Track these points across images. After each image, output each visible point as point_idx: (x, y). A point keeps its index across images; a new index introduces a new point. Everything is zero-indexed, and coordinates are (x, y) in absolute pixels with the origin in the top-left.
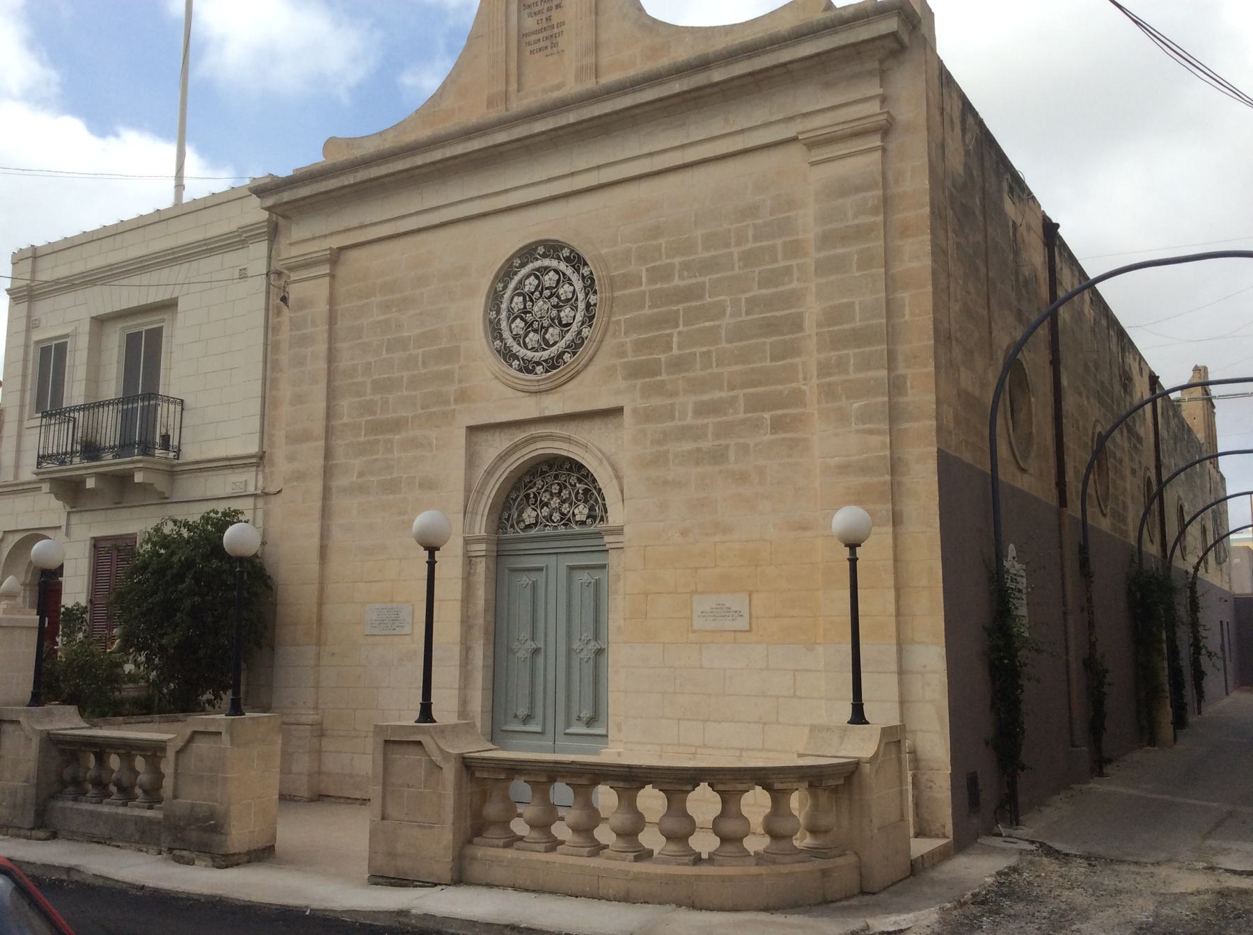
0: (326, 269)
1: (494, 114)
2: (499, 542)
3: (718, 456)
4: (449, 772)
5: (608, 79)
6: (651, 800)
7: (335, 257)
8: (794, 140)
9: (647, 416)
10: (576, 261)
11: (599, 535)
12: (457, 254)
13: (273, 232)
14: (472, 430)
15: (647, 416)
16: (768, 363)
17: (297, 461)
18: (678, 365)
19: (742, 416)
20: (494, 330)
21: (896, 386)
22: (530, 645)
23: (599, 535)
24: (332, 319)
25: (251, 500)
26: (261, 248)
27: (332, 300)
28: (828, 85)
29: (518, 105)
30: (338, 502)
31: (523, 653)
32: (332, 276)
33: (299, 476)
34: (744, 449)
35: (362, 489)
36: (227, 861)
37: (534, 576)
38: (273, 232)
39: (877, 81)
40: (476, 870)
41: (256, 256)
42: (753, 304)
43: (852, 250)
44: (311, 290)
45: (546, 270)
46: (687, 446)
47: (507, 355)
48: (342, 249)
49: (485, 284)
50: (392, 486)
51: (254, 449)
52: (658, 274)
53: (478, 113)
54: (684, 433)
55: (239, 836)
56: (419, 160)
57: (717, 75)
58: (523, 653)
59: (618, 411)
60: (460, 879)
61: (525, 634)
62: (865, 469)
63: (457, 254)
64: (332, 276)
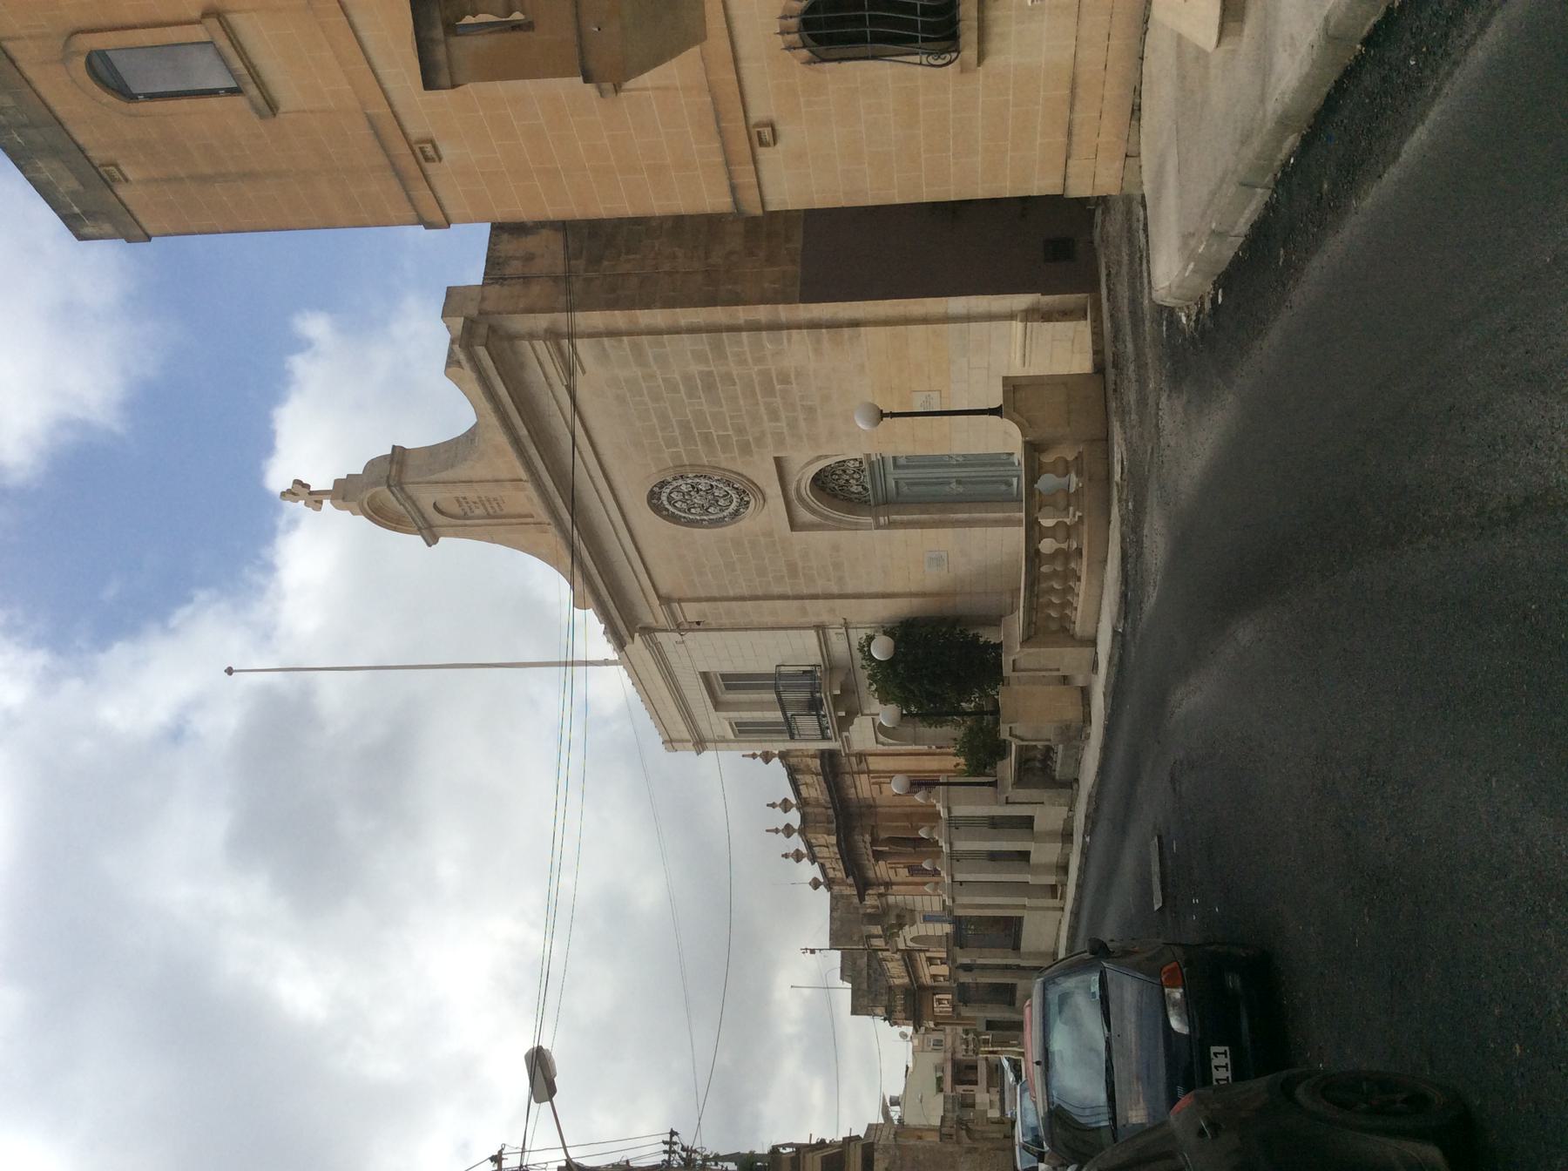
0: (675, 605)
1: (553, 530)
2: (877, 505)
3: (810, 410)
4: (1027, 650)
5: (523, 474)
6: (1047, 546)
7: (665, 600)
8: (568, 387)
9: (780, 441)
10: (663, 484)
11: (871, 464)
12: (663, 551)
13: (647, 631)
14: (794, 526)
15: (780, 441)
16: (738, 388)
17: (819, 611)
18: (740, 430)
19: (778, 399)
20: (719, 523)
21: (754, 327)
22: (954, 485)
23: (871, 464)
24: (708, 599)
25: (851, 631)
26: (660, 637)
27: (698, 600)
28: (522, 366)
29: (543, 516)
30: (849, 590)
31: (961, 489)
32: (680, 601)
33: (832, 611)
34: (802, 398)
35: (841, 579)
36: (1087, 719)
37: (902, 483)
38: (647, 631)
39: (517, 342)
40: (1089, 631)
41: (667, 640)
42: (690, 396)
43: (649, 354)
44: (691, 612)
45: (669, 499)
46: (802, 424)
47: (736, 514)
48: (659, 597)
49: (682, 530)
50: (837, 566)
51: (813, 633)
52: (671, 443)
53: (552, 537)
54: (792, 425)
55: (1072, 713)
56: (594, 571)
57: (523, 432)
58: (961, 489)
59: (779, 462)
60: (1093, 642)
61: (947, 488)
62: (818, 341)
63: (663, 551)
64: (680, 601)
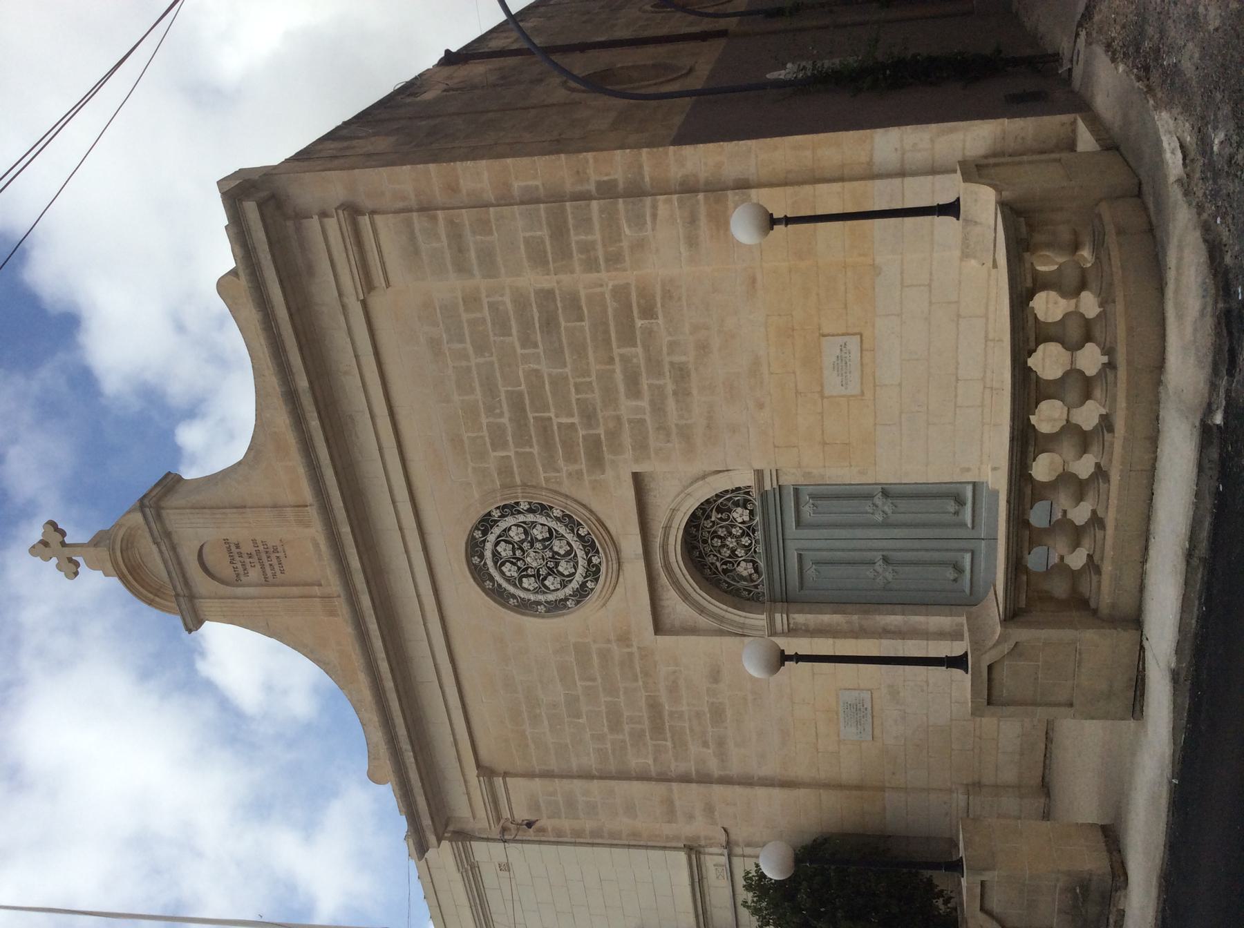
0: (499, 781)
1: (342, 606)
2: (773, 600)
3: (681, 374)
4: (1022, 634)
5: (307, 494)
7: (486, 772)
8: (364, 303)
9: (641, 447)
10: (486, 523)
11: (764, 495)
13: (462, 836)
14: (658, 629)
15: (641, 447)
16: (586, 324)
17: (694, 813)
18: (589, 417)
19: (640, 350)
20: (557, 607)
21: (607, 191)
23: (764, 495)
24: (548, 775)
25: (736, 860)
26: (478, 848)
27: (530, 775)
28: (311, 270)
29: (334, 585)
30: (735, 769)
32: (505, 775)
33: (709, 810)
34: (673, 346)
35: (721, 743)
36: (1119, 873)
37: (808, 564)
38: (462, 836)
39: (305, 221)
41: (486, 854)
42: (526, 341)
44: (520, 797)
45: (496, 554)
46: (671, 404)
47: (582, 593)
48: (479, 765)
50: (718, 714)
51: (682, 857)
52: (498, 440)
53: (343, 627)
54: (658, 408)
55: (1093, 861)
56: (389, 684)
57: (303, 383)
59: (637, 477)
60: (1135, 621)
62: (693, 220)
64: (505, 775)
